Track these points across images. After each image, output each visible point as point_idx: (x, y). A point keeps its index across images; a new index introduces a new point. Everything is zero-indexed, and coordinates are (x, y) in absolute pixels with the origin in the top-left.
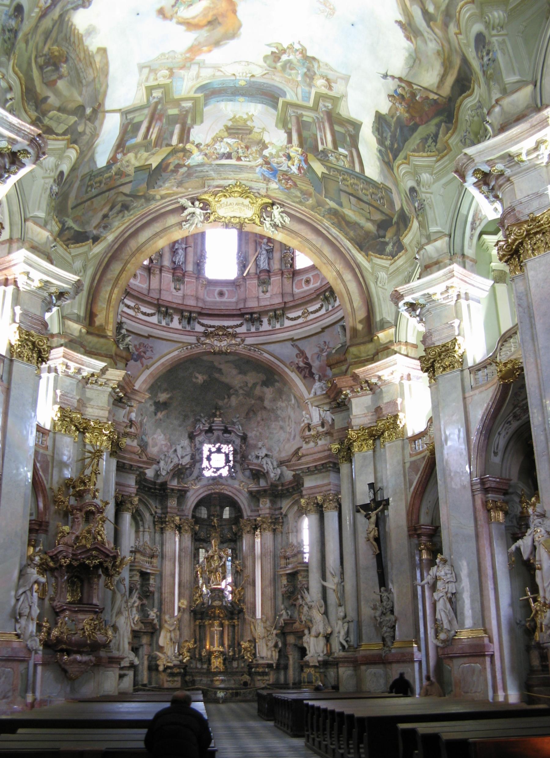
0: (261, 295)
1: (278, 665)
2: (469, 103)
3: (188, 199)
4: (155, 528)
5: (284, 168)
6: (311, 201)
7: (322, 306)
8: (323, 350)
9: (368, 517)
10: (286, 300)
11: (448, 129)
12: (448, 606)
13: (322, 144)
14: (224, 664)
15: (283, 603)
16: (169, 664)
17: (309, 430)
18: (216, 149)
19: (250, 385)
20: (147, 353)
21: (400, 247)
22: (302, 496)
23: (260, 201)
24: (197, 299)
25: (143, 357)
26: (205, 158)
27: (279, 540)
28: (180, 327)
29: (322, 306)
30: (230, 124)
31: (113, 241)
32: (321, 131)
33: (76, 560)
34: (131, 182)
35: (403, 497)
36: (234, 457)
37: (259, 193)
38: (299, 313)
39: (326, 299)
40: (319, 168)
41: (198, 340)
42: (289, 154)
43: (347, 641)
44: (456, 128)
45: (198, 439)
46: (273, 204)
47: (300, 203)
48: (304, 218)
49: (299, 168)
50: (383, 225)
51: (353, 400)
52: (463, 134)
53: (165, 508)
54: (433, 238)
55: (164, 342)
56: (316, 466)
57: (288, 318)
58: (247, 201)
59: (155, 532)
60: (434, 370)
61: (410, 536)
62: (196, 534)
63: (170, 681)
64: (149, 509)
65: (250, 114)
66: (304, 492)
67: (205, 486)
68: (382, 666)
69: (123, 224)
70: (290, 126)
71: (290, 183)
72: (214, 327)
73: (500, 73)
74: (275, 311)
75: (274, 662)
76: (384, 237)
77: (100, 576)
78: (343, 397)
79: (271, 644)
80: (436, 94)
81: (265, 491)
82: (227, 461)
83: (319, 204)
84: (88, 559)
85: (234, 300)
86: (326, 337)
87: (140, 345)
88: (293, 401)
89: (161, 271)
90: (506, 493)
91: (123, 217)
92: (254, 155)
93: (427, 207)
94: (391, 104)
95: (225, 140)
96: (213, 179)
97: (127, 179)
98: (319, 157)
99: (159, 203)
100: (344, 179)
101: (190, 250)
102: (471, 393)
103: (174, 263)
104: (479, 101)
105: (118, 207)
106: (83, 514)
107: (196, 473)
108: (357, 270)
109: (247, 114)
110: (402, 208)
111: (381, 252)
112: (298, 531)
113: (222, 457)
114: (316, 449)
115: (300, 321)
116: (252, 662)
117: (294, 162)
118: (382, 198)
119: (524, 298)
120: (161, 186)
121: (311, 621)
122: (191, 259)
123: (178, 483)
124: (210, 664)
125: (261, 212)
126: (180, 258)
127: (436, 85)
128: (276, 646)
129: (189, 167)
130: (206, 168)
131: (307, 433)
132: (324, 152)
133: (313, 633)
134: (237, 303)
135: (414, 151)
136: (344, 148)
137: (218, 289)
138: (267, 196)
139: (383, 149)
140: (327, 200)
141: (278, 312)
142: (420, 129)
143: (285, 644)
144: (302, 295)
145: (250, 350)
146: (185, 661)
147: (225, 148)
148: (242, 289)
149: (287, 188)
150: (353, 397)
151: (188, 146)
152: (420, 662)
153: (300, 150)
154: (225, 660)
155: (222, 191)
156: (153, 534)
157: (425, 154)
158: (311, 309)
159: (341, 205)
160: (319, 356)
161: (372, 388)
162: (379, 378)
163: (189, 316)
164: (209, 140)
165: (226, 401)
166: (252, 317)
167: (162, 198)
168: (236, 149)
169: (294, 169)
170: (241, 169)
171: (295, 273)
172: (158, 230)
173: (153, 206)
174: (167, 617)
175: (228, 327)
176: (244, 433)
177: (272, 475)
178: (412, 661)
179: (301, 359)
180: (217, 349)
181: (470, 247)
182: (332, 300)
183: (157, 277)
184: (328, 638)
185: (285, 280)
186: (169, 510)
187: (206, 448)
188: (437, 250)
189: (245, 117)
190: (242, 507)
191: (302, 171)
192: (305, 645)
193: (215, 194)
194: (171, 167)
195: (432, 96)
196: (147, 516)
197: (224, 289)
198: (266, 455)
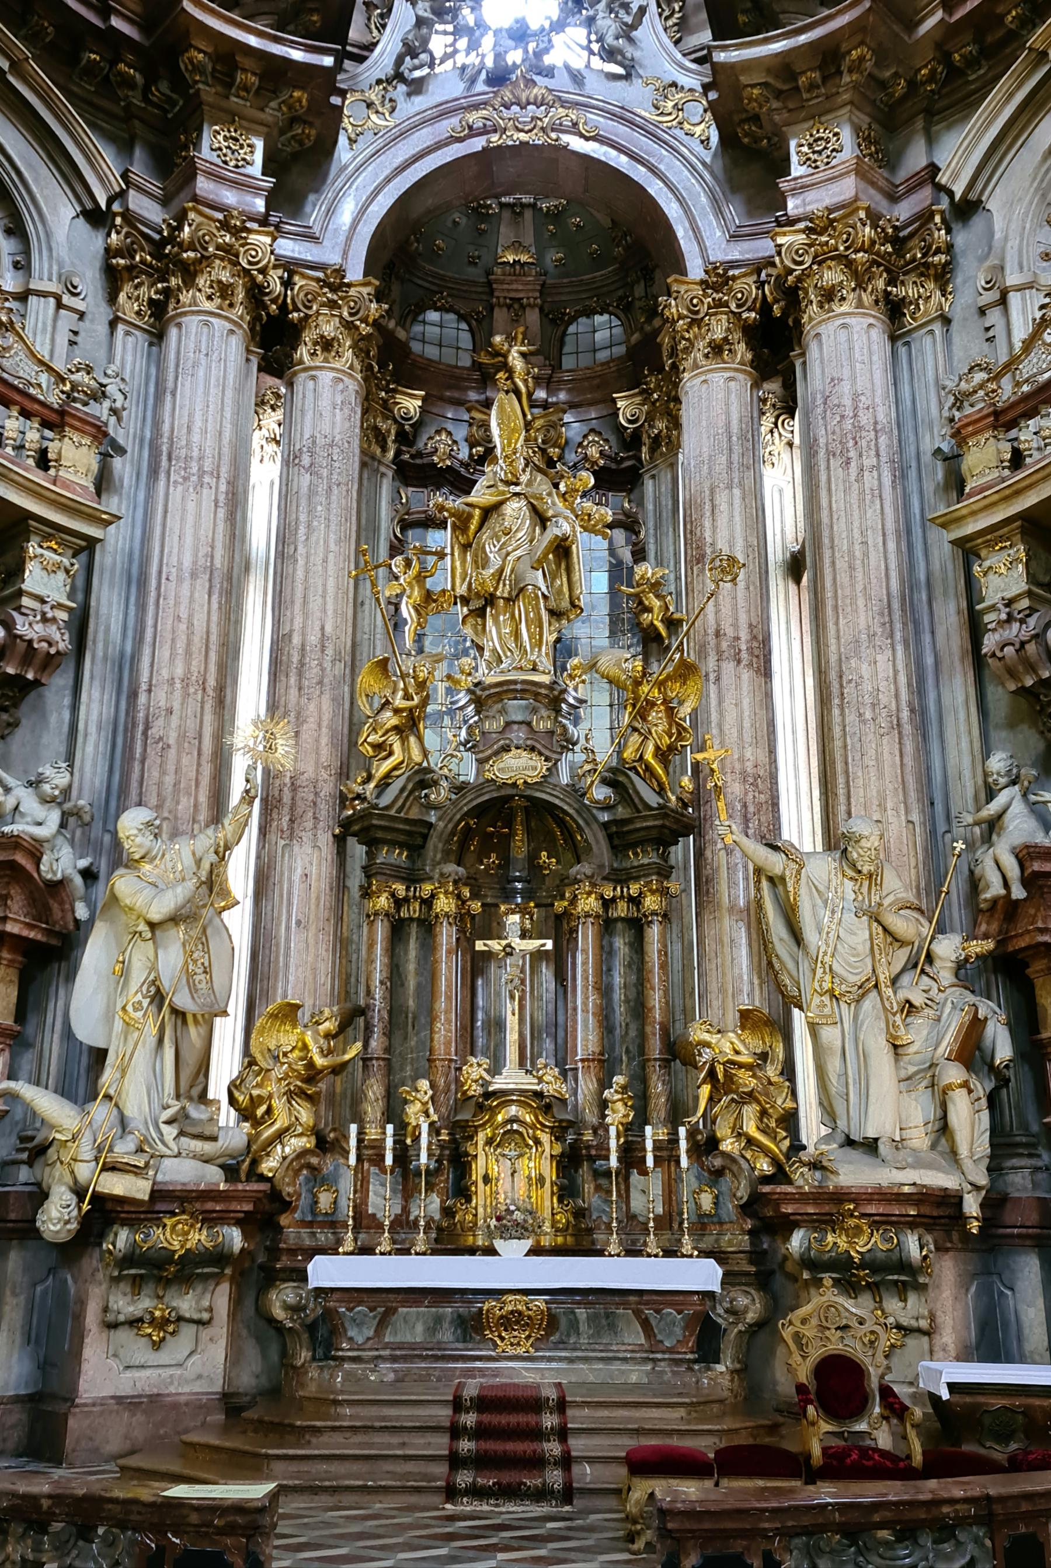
4: (112, 298)
16: (116, 1185)
53: (175, 170)
59: (113, 324)
62: (405, 438)
63: (134, 1323)
64: (70, 175)
67: (444, 111)
79: (934, 1036)
116: (780, 1175)
124: (462, 1191)
128: (971, 1051)
146: (269, 1165)
154: (571, 1161)
156: (103, 329)
186: (203, 185)
190: (672, 210)
196: (58, 214)
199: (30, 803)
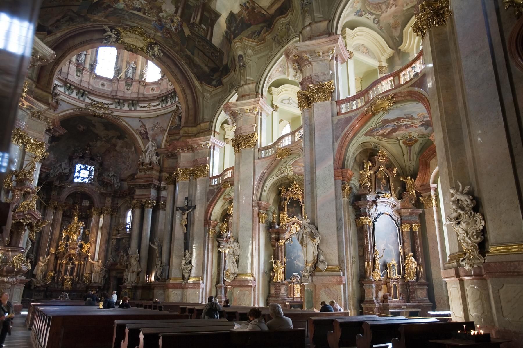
0: (126, 91)
1: (104, 287)
2: (283, 21)
3: (109, 27)
5: (168, 26)
6: (177, 48)
7: (159, 104)
9: (183, 214)
10: (140, 96)
11: (267, 31)
12: (234, 261)
13: (194, 19)
14: (72, 285)
15: (111, 254)
16: (38, 285)
17: (143, 166)
18: (133, 4)
19: (110, 137)
21: (220, 83)
22: (134, 199)
23: (148, 40)
24: (89, 84)
27: (114, 220)
28: (77, 97)
29: (159, 104)
31: (59, 37)
32: (195, 13)
33: (15, 220)
34: (78, 5)
35: (204, 205)
36: (94, 174)
38: (146, 105)
39: (163, 101)
40: (187, 32)
43: (161, 276)
44: (271, 31)
45: (74, 161)
46: (156, 44)
47: (171, 47)
48: (170, 55)
49: (176, 29)
50: (214, 70)
51: (182, 154)
52: (274, 35)
54: (248, 82)
55: (66, 104)
56: (144, 185)
57: (139, 106)
58: (141, 38)
60: (239, 146)
61: (205, 225)
66: (135, 197)
68: (181, 289)
69: (68, 29)
70: (179, 4)
72: (96, 102)
73: (313, 10)
74: (133, 101)
75: (102, 285)
76: (213, 76)
77: (26, 230)
78: (176, 151)
80: (266, 11)
81: (110, 194)
82: (90, 174)
83: (182, 51)
84: (23, 219)
85: (110, 90)
86: (159, 120)
88: (133, 149)
89: (70, 63)
90: (266, 211)
91: (69, 25)
93: (247, 67)
94: (240, 10)
96: (126, 20)
97: (77, 3)
98: (189, 26)
100: (199, 41)
101: (89, 57)
102: (258, 160)
103: (78, 61)
104: (289, 22)
105: (67, 18)
106: (23, 193)
107: (70, 178)
108: (193, 90)
110: (227, 64)
111: (209, 83)
112: (125, 217)
113: (87, 172)
114: (145, 176)
115: (146, 109)
118: (217, 56)
119: (308, 120)
120: (95, 14)
121: (130, 264)
122: (88, 61)
123: (59, 183)
125: (148, 46)
126: (82, 58)
127: (267, 7)
128: (104, 277)
129: (115, 9)
130: (124, 13)
131: (141, 167)
132: (193, 24)
133: (131, 271)
134: (111, 92)
135: (246, 37)
136: (205, 25)
137: (101, 82)
138: (154, 39)
139: (229, 32)
140: (186, 50)
141: (134, 102)
142: (252, 27)
143: (109, 277)
144: (149, 96)
148: (116, 85)
149: (166, 38)
150: (182, 152)
152: (203, 289)
153: (180, 19)
155: (129, 29)
157: (252, 40)
158: (153, 104)
159: (193, 54)
160: (153, 129)
161: (193, 150)
162: (199, 146)
163: (82, 92)
165: (94, 143)
166: (120, 101)
167: (95, 21)
169: (173, 29)
170: (144, 19)
171: (146, 84)
172: (88, 39)
173: (88, 24)
174: (41, 258)
175: (105, 104)
176: (102, 162)
177: (116, 186)
178: (199, 287)
181: (265, 91)
182: (165, 102)
183: (67, 66)
184: (138, 274)
185: (141, 86)
186: (52, 197)
187: (78, 167)
188: (249, 89)
192: (125, 277)
193: (125, 29)
194: (105, 5)
195: (263, 12)
197: (105, 83)
198: (114, 175)
199: (31, 255)
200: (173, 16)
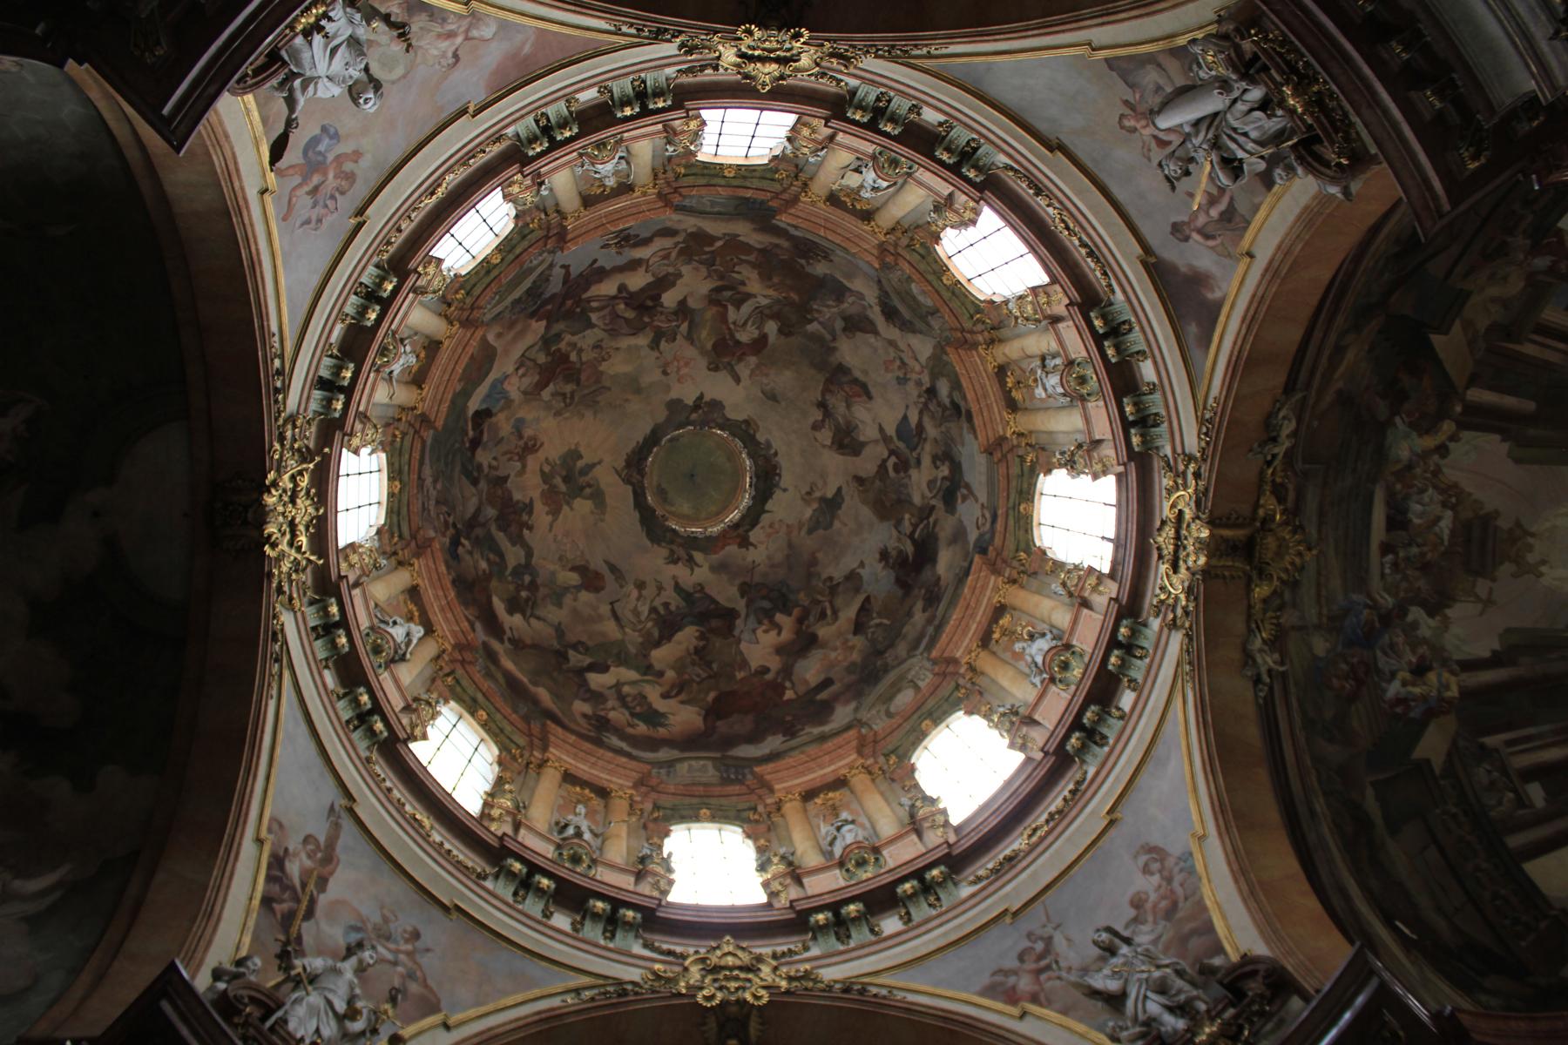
5: (1382, 662)
8: (388, 938)
13: (1510, 743)
18: (1422, 491)
20: (309, 201)
25: (306, 179)
26: (1399, 467)
30: (1504, 523)
37: (1281, 608)
40: (1433, 745)
41: (292, 419)
42: (1430, 668)
49: (1401, 701)
55: (315, 281)
65: (1543, 569)
71: (1349, 685)
86: (437, 932)
87: (351, 177)
92: (1404, 585)
95: (1449, 513)
99: (1333, 337)
109: (1544, 562)
117: (1414, 685)
140: (1370, 793)
145: (275, 639)
147: (1421, 516)
151: (1448, 427)
153: (1454, 692)
164: (1450, 474)
167: (1339, 350)
168: (1420, 540)
169: (1394, 689)
179: (308, 863)
180: (270, 500)
189: (1531, 558)
191: (1399, 710)
200: (1445, 663)
